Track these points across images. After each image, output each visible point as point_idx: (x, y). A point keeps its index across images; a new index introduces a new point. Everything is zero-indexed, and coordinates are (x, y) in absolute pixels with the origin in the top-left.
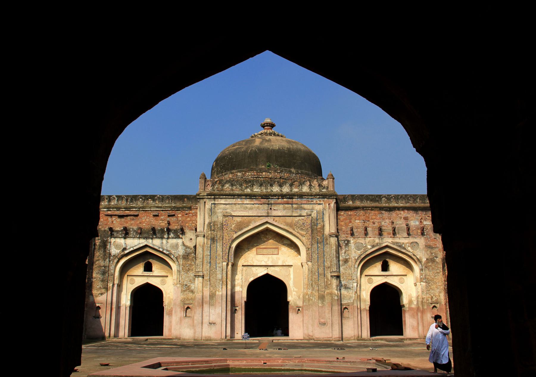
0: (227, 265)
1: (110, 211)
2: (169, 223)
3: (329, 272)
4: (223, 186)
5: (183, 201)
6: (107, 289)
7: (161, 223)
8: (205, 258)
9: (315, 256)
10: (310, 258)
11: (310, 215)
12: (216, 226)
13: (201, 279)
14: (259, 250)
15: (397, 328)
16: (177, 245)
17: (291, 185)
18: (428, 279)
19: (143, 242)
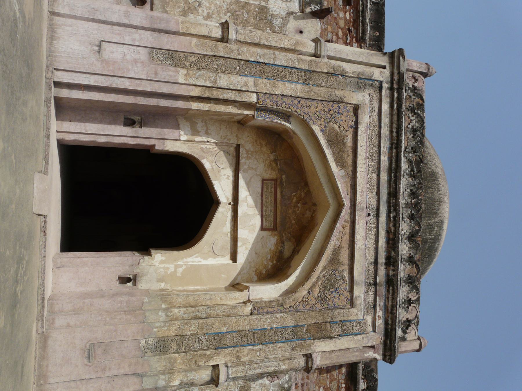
0: (248, 106)
3: (228, 359)
4: (413, 110)
8: (268, 51)
9: (266, 322)
13: (217, 33)
14: (270, 184)
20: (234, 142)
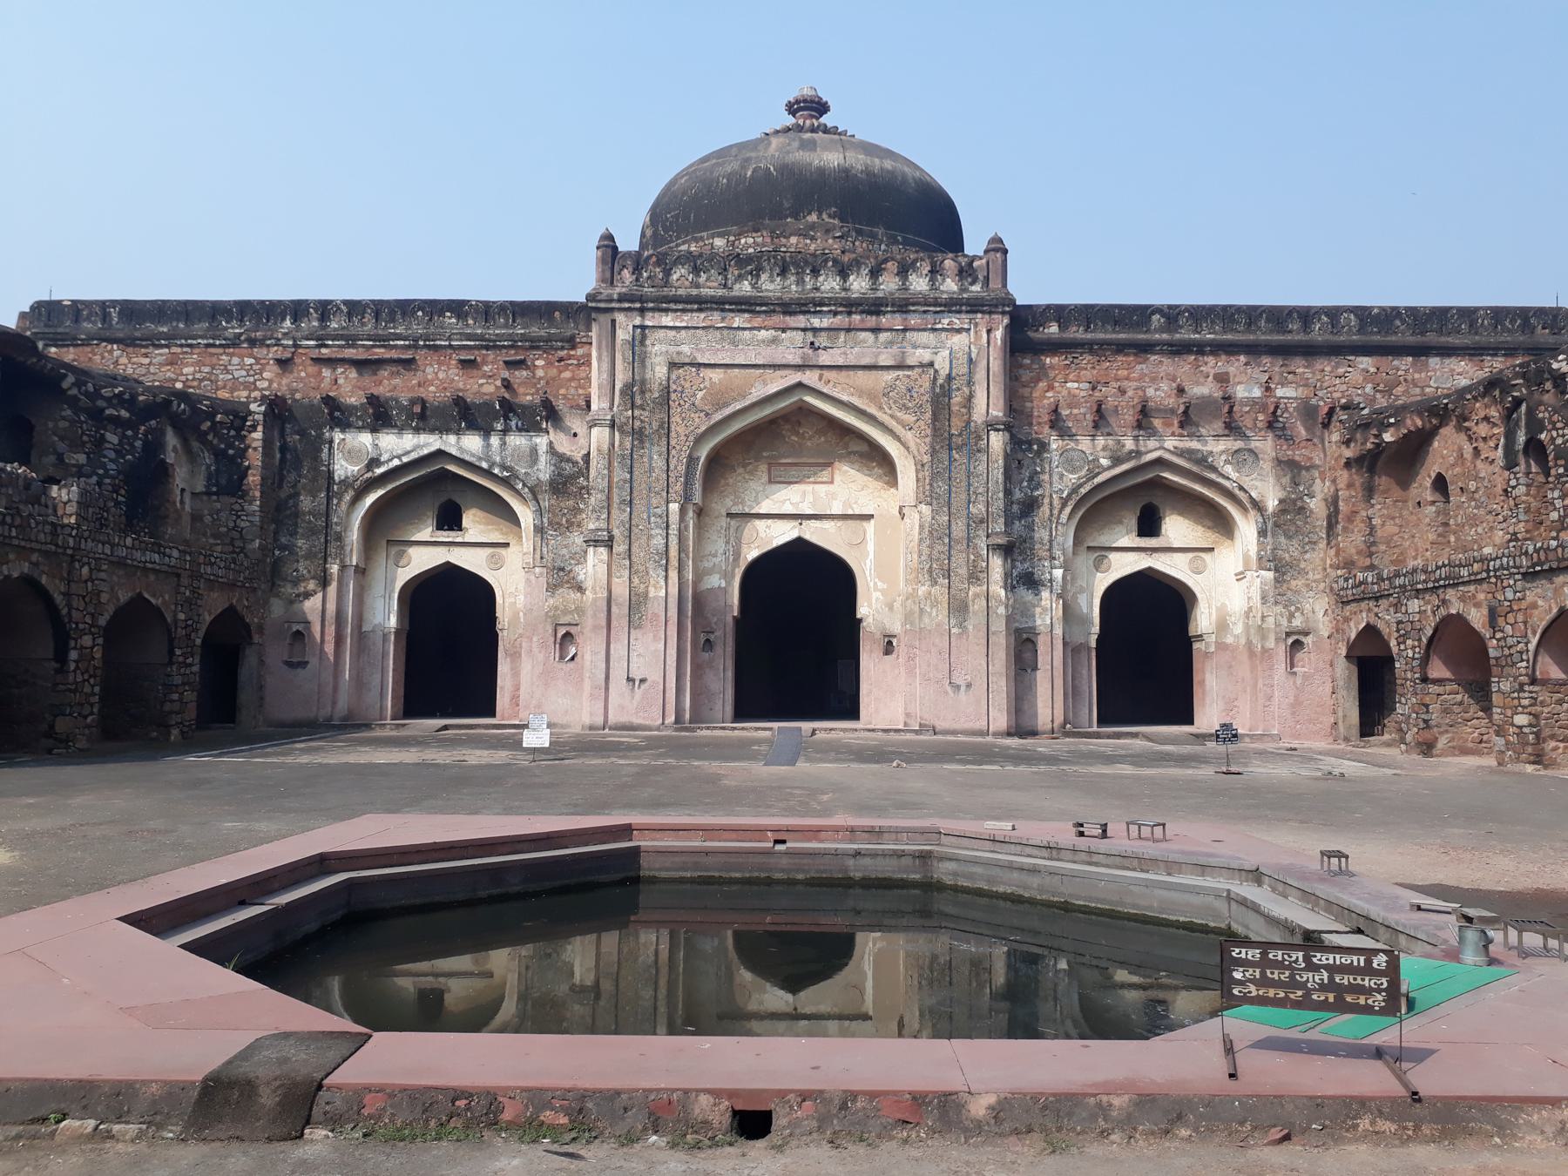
1: (326, 346)
2: (507, 385)
3: (982, 533)
4: (667, 273)
5: (551, 318)
6: (324, 582)
7: (483, 387)
10: (927, 495)
11: (931, 364)
12: (648, 395)
13: (603, 551)
15: (1176, 703)
16: (534, 451)
17: (875, 273)
18: (1281, 560)
19: (430, 442)
20: (724, 522)
